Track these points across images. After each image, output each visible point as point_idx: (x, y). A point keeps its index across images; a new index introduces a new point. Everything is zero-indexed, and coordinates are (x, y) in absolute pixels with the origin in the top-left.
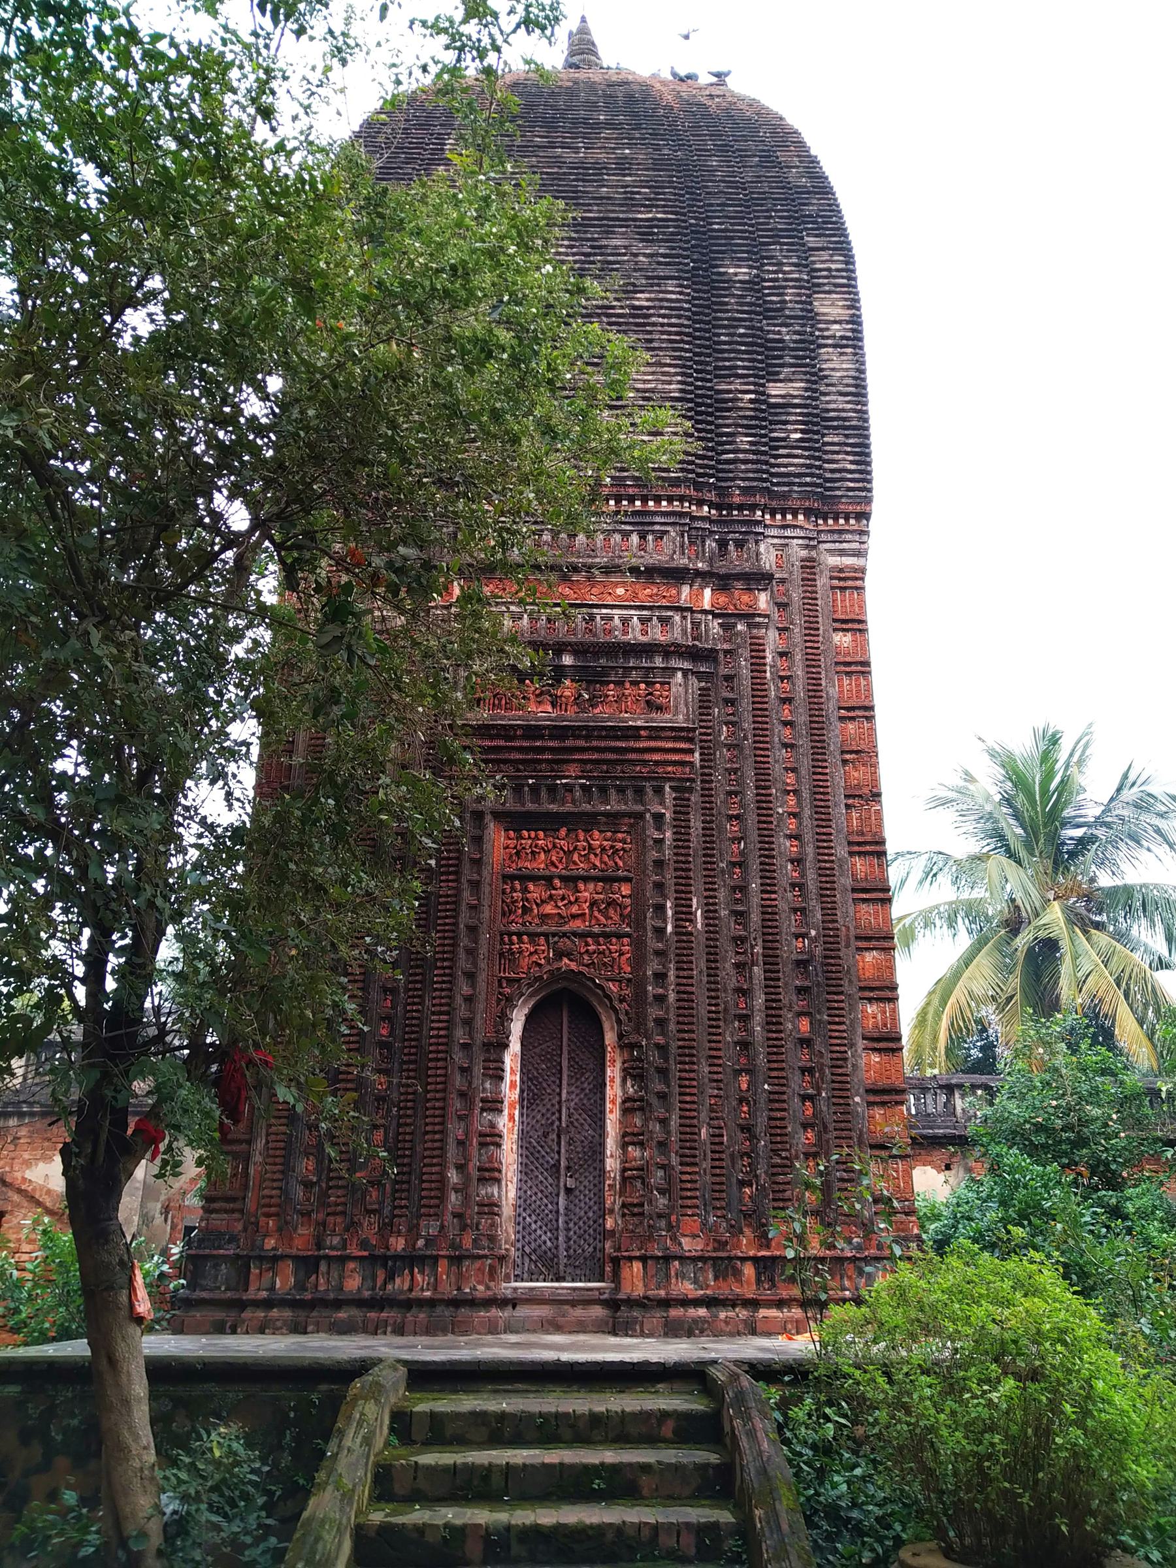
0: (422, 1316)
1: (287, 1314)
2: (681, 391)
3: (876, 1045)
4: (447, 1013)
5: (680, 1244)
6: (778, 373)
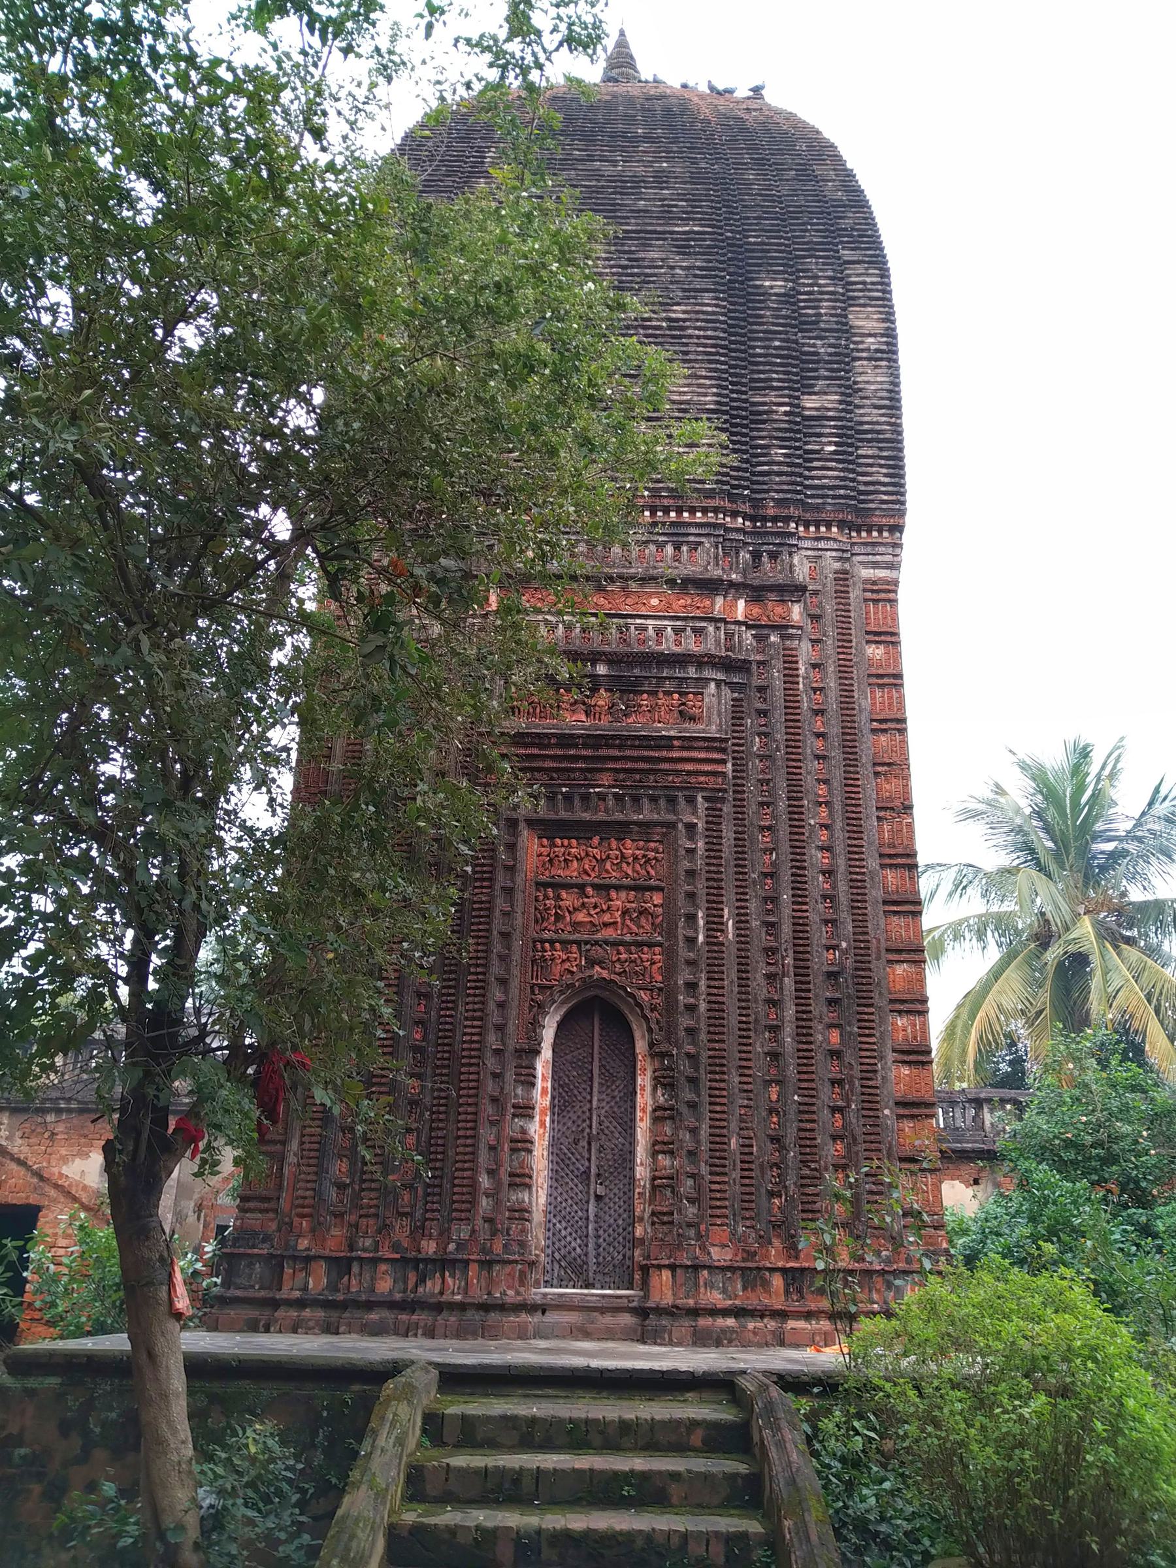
0: (453, 1319)
1: (320, 1314)
2: (718, 403)
3: (906, 1058)
4: (481, 1019)
6: (813, 386)
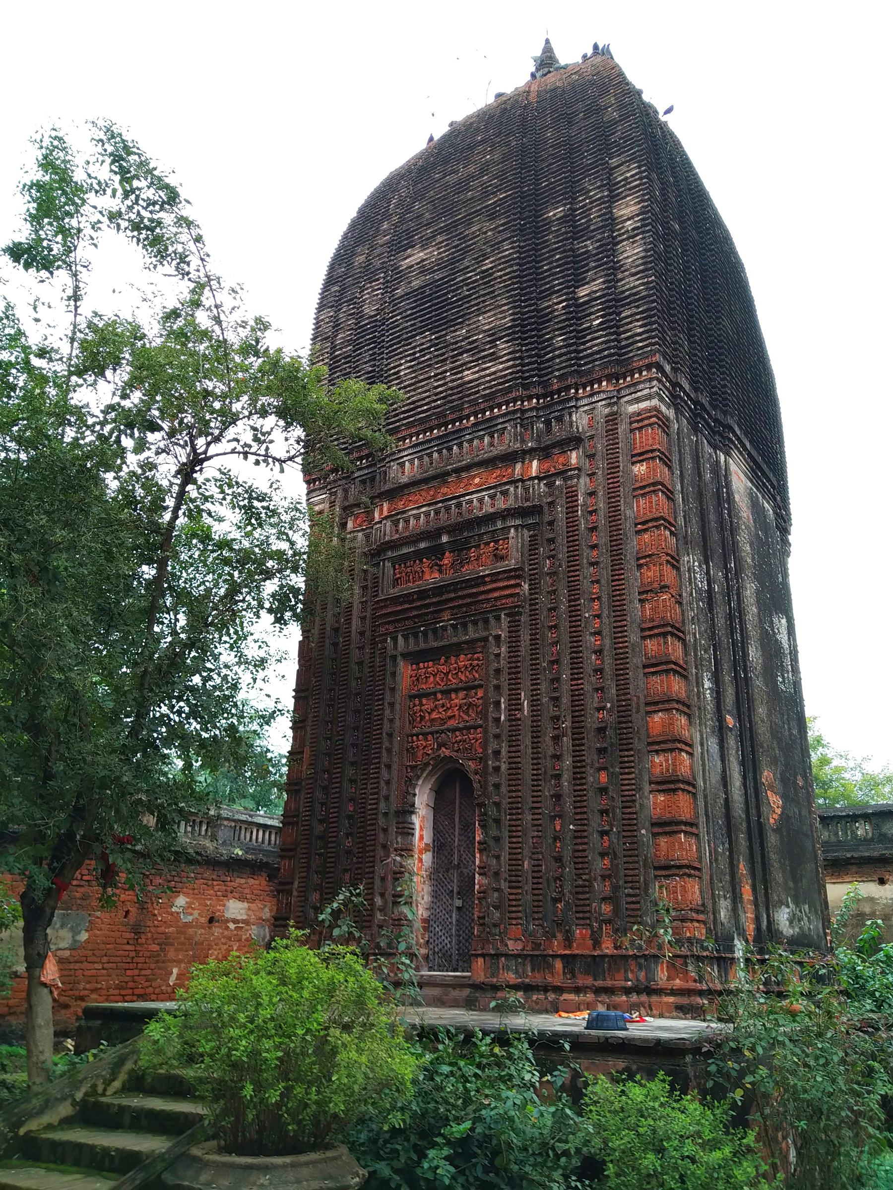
2: (513, 320)
3: (660, 788)
5: (506, 945)
6: (585, 278)
